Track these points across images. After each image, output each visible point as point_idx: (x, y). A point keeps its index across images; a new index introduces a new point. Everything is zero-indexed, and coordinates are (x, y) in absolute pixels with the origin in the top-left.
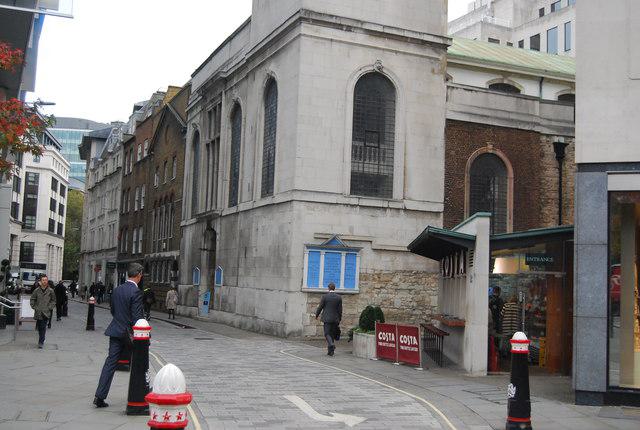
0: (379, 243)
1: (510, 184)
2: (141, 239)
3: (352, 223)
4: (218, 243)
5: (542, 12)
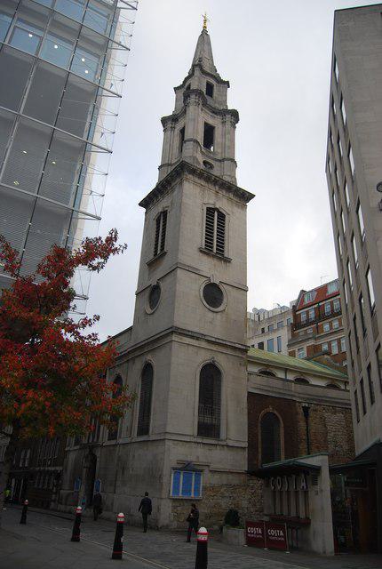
0: (213, 466)
1: (282, 431)
2: (28, 456)
3: (198, 454)
4: (98, 464)
5: (263, 330)
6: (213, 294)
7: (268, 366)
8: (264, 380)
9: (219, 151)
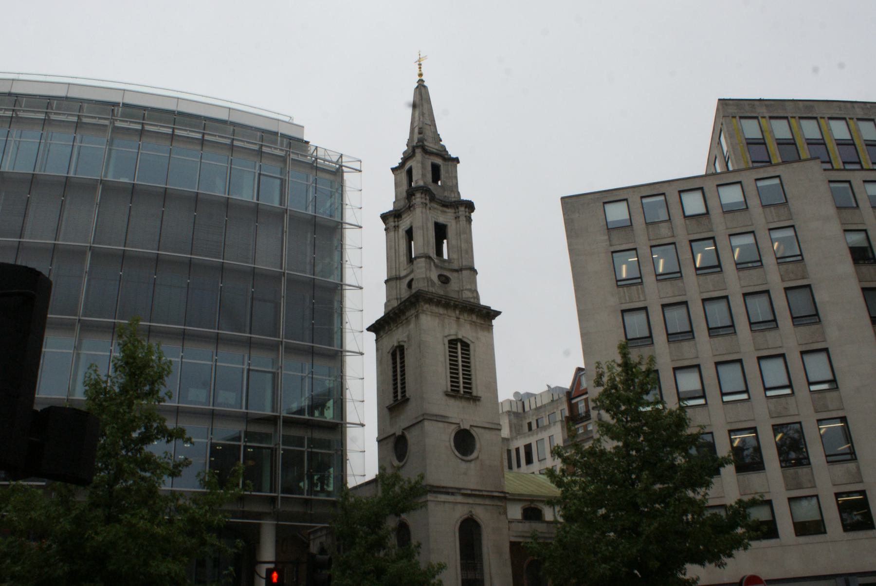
5: (530, 424)
6: (464, 442)
7: (532, 501)
8: (527, 527)
9: (455, 256)
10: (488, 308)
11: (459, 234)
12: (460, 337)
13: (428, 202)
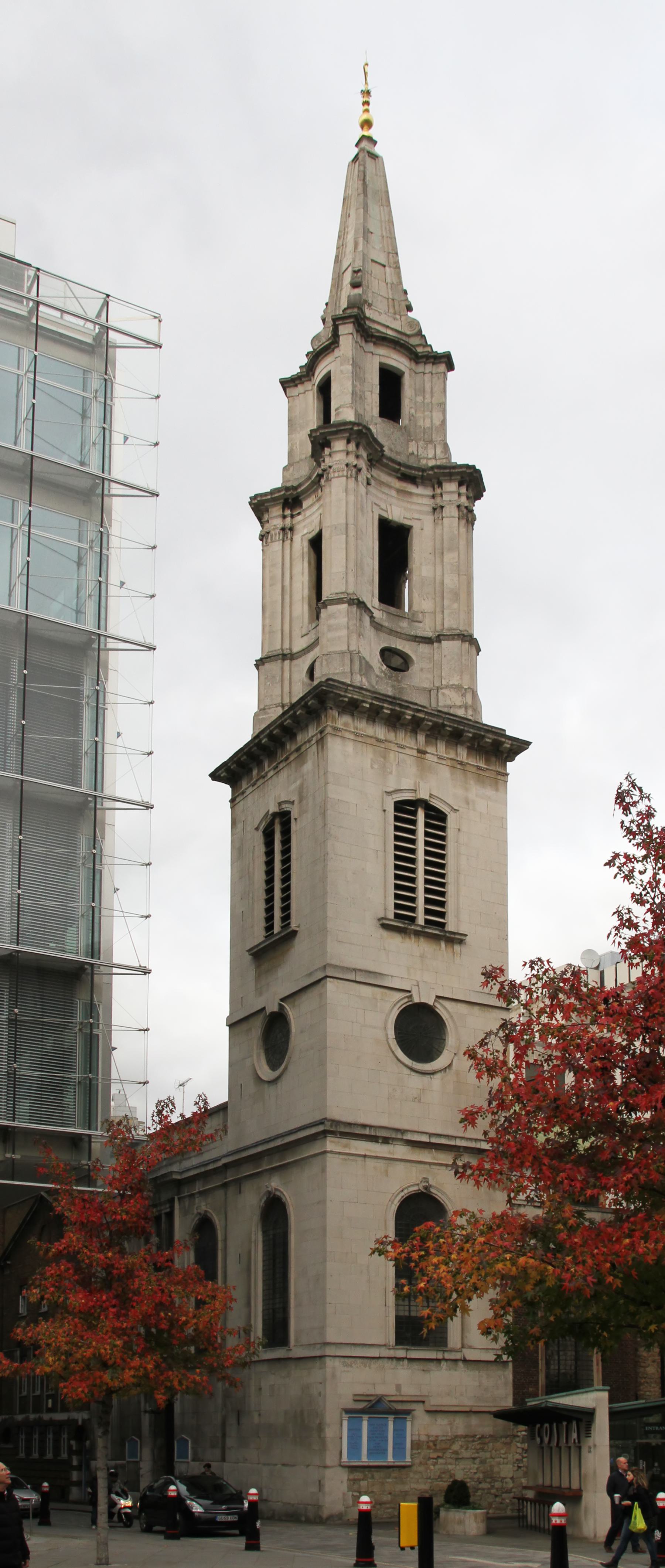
10: (499, 733)
11: (439, 552)
12: (424, 795)
13: (362, 464)
